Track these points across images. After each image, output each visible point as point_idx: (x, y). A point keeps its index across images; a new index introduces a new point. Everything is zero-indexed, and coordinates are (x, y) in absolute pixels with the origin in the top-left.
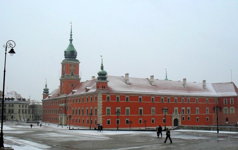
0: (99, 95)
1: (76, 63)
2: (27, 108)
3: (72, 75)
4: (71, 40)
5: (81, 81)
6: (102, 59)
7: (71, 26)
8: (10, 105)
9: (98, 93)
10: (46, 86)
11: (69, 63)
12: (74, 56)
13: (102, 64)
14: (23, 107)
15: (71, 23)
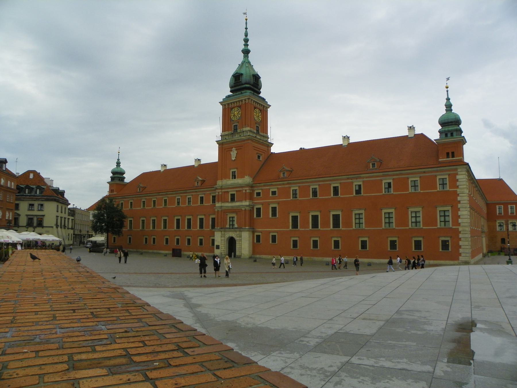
0: (459, 173)
1: (264, 106)
2: (66, 216)
3: (258, 131)
4: (246, 52)
5: (274, 150)
6: (447, 88)
7: (246, 20)
8: (32, 205)
9: (456, 170)
10: (118, 164)
11: (254, 101)
12: (257, 88)
13: (448, 99)
14: (62, 212)
15: (245, 14)
